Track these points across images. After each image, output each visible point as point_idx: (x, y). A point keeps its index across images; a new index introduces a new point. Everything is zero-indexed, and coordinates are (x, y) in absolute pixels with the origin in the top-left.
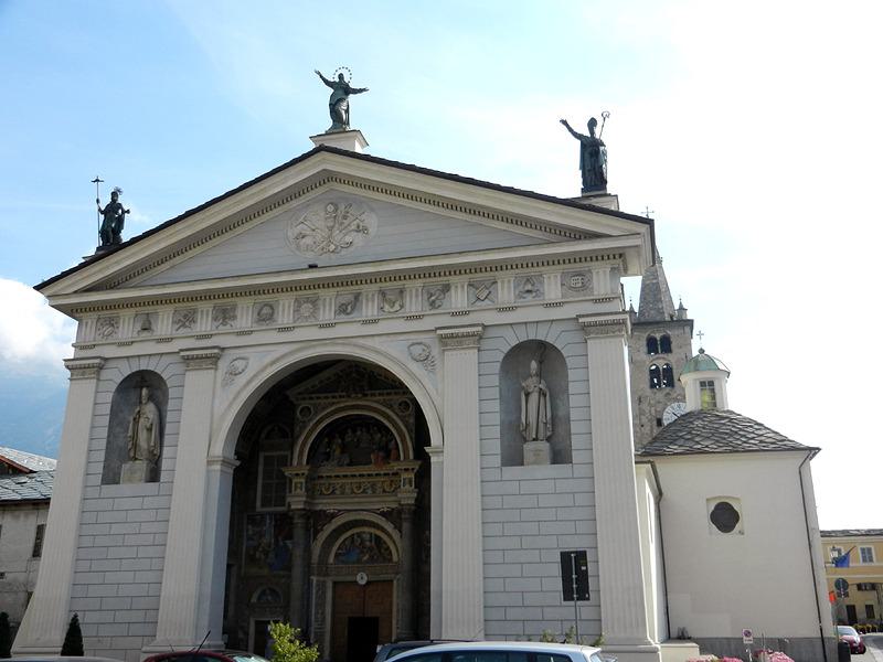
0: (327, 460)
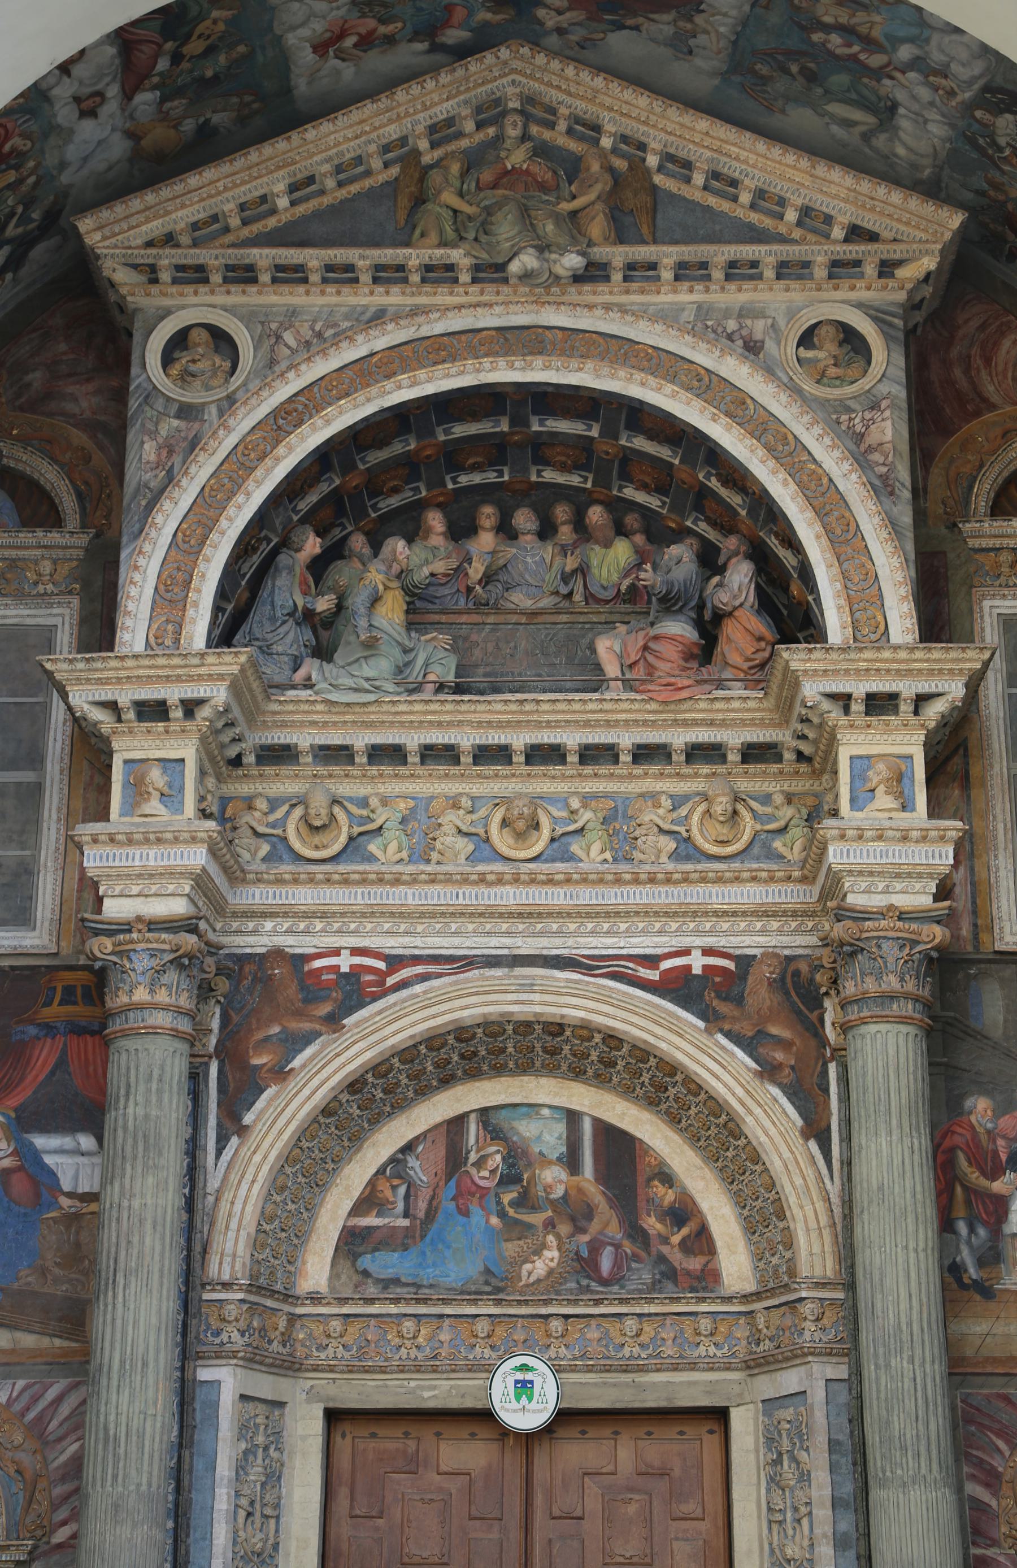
0: (323, 652)
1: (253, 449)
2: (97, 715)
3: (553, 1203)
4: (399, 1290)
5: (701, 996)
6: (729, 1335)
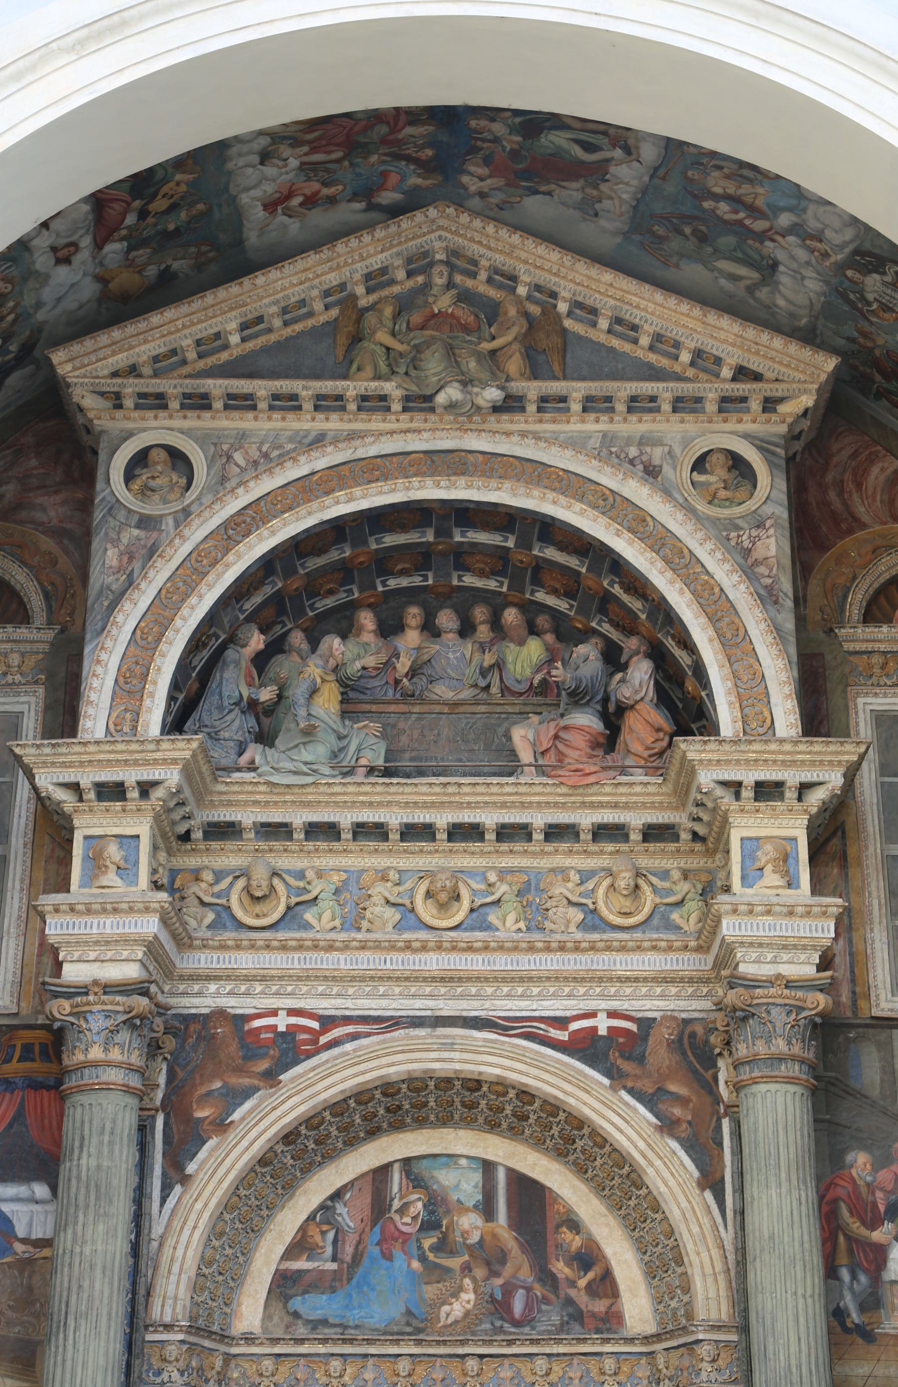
0: (265, 738)
1: (205, 556)
2: (61, 795)
3: (469, 1248)
4: (326, 1331)
5: (606, 1055)
6: (631, 1375)
